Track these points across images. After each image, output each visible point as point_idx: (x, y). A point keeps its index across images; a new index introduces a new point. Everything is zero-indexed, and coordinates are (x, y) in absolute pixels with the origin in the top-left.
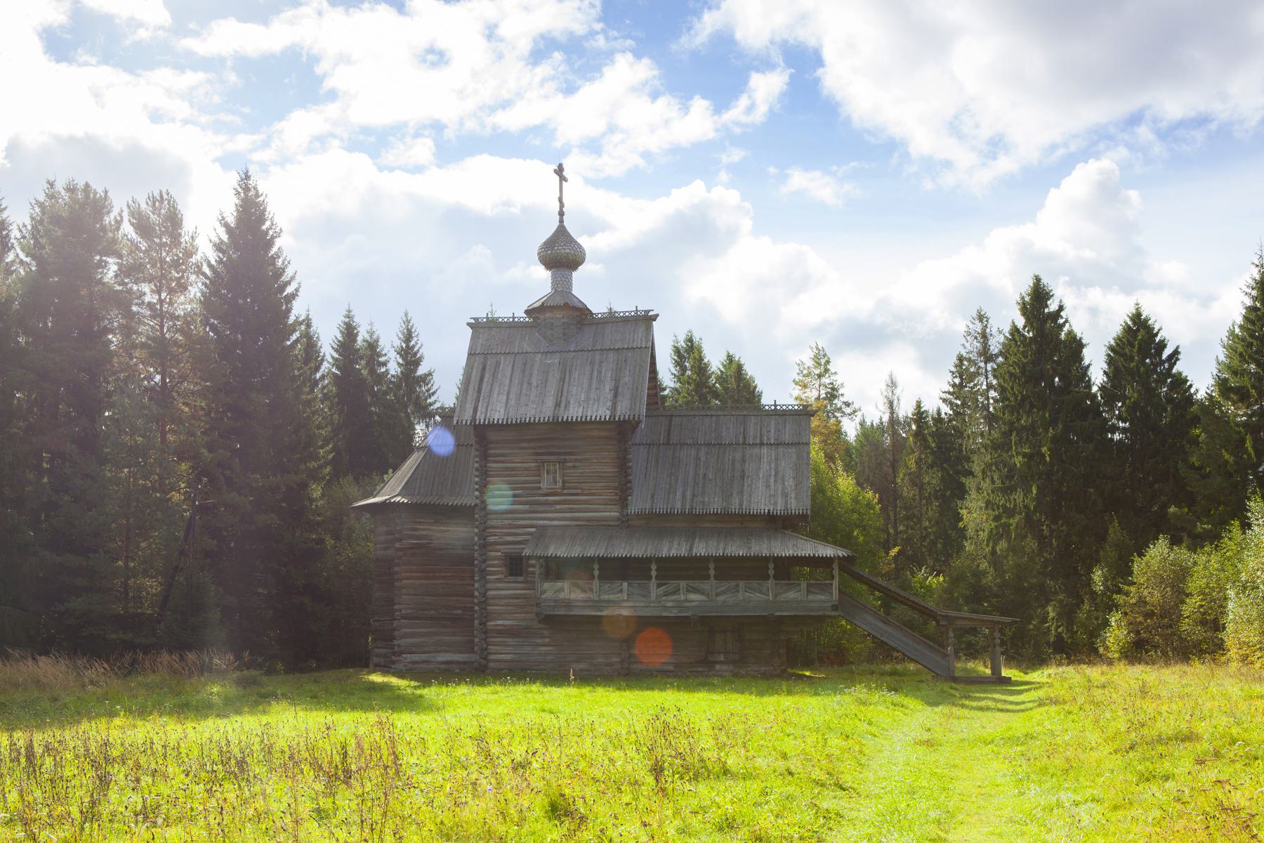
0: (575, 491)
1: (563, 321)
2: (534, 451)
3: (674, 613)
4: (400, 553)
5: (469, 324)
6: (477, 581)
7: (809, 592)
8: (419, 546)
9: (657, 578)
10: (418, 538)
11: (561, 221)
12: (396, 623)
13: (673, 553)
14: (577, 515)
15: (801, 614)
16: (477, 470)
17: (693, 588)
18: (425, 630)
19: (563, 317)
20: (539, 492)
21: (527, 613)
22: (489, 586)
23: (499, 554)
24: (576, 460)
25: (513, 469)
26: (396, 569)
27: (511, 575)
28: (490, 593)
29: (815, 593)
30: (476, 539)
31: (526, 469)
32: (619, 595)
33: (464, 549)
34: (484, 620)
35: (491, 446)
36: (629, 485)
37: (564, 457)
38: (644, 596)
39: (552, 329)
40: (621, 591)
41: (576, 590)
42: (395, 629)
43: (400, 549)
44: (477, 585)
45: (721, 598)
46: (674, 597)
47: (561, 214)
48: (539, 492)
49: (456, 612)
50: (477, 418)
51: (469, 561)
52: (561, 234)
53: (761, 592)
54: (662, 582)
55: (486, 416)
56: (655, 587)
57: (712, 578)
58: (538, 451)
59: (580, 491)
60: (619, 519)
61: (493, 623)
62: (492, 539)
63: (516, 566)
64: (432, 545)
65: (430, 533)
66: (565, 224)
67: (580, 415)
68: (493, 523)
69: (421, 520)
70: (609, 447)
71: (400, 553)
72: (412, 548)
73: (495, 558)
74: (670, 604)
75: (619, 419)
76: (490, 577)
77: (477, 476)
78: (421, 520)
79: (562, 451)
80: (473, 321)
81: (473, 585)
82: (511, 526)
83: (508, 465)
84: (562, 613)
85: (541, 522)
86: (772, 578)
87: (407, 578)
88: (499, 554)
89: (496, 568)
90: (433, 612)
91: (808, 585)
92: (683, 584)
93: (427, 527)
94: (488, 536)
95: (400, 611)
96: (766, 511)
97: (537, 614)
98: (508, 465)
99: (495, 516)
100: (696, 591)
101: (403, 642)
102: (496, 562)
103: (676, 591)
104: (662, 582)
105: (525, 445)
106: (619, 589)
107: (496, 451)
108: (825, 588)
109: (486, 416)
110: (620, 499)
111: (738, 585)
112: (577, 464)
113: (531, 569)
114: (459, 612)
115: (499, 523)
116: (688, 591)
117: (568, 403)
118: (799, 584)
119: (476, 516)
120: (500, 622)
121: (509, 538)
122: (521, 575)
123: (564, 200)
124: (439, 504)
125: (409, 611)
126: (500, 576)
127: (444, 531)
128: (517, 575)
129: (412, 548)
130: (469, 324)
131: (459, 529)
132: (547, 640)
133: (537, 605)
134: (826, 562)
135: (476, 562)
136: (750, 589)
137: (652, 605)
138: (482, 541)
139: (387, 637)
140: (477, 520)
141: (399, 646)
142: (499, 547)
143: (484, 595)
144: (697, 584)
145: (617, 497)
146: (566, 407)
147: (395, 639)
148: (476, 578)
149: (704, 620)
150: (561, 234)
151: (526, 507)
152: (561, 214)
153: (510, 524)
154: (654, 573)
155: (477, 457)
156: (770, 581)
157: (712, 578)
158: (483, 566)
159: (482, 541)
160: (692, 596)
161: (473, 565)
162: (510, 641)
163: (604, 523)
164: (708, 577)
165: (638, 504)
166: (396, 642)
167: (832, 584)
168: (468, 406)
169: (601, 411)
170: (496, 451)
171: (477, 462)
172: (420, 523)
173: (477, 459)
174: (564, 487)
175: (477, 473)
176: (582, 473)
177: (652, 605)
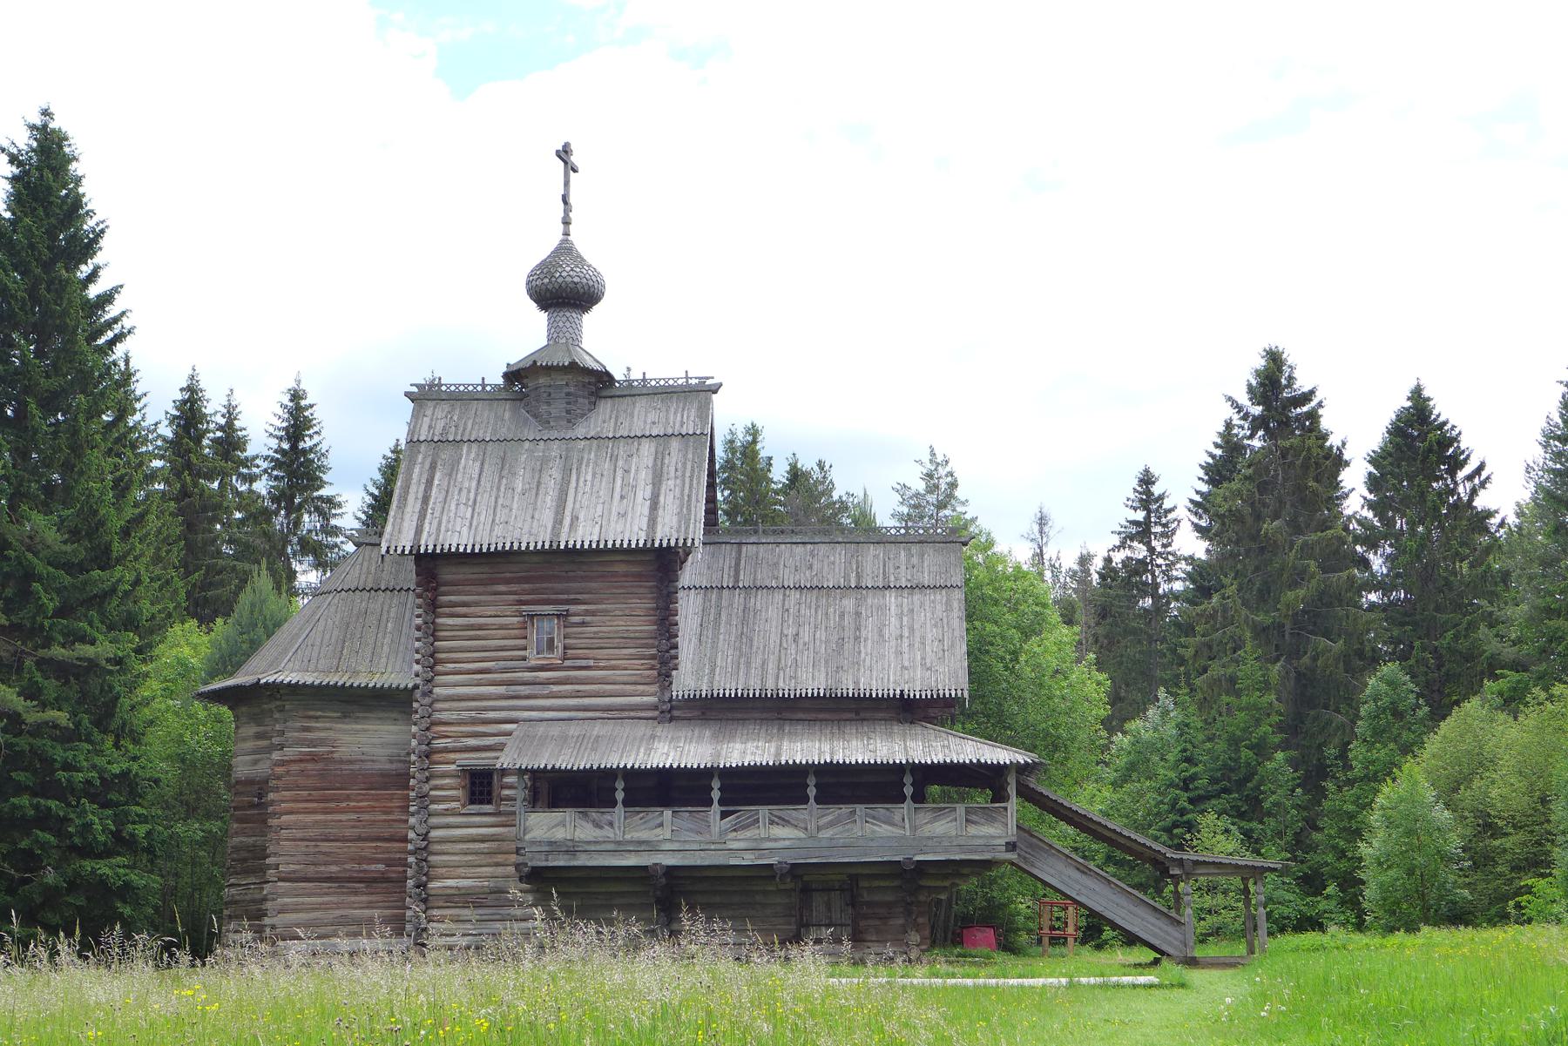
0: (583, 663)
1: (566, 390)
2: (516, 597)
3: (748, 859)
4: (280, 770)
5: (407, 394)
6: (413, 814)
8: (314, 758)
9: (721, 802)
10: (312, 743)
11: (566, 234)
12: (267, 888)
13: (748, 760)
14: (587, 701)
15: (957, 857)
16: (418, 628)
17: (780, 818)
18: (320, 900)
19: (567, 385)
21: (497, 865)
22: (434, 821)
23: (453, 767)
24: (587, 613)
25: (480, 627)
27: (472, 802)
28: (434, 834)
30: (414, 743)
31: (502, 627)
32: (658, 831)
33: (391, 762)
34: (424, 878)
35: (443, 589)
36: (673, 652)
37: (567, 607)
39: (549, 404)
40: (661, 825)
41: (584, 824)
42: (265, 899)
43: (282, 763)
46: (748, 834)
47: (566, 222)
49: (373, 867)
50: (423, 542)
51: (400, 780)
53: (893, 825)
54: (732, 808)
55: (437, 539)
56: (718, 817)
57: (812, 800)
58: (524, 597)
59: (591, 663)
60: (655, 708)
61: (439, 884)
62: (440, 743)
63: (481, 786)
64: (335, 755)
65: (331, 734)
67: (595, 538)
68: (444, 716)
69: (319, 713)
70: (642, 590)
71: (280, 770)
72: (301, 761)
73: (444, 775)
75: (661, 544)
76: (435, 806)
77: (418, 640)
78: (319, 713)
80: (415, 389)
82: (474, 722)
83: (472, 621)
84: (562, 863)
85: (526, 714)
87: (291, 813)
88: (453, 767)
89: (449, 792)
90: (334, 868)
91: (968, 811)
93: (328, 725)
94: (434, 738)
95: (277, 866)
96: (898, 692)
97: (517, 866)
98: (472, 621)
100: (785, 822)
101: (279, 920)
102: (447, 781)
104: (732, 808)
105: (502, 588)
106: (658, 821)
107: (452, 598)
109: (437, 539)
110: (659, 675)
112: (588, 619)
113: (506, 792)
114: (381, 867)
115: (454, 716)
116: (772, 822)
117: (575, 519)
119: (415, 705)
120: (450, 883)
121: (472, 742)
122: (489, 802)
123: (572, 200)
124: (351, 686)
125: (292, 867)
126: (454, 805)
127: (358, 731)
128: (481, 802)
129: (301, 761)
130: (407, 394)
133: (518, 851)
134: (998, 770)
135: (412, 782)
136: (874, 818)
138: (424, 747)
139: (255, 914)
141: (273, 927)
142: (452, 756)
143: (425, 837)
144: (788, 811)
145: (655, 673)
146: (571, 525)
147: (266, 915)
148: (412, 809)
149: (796, 871)
150: (565, 249)
151: (501, 690)
152: (566, 222)
154: (716, 795)
155: (419, 607)
156: (905, 805)
157: (812, 800)
158: (426, 787)
159: (424, 747)
160: (778, 831)
161: (407, 787)
162: (466, 913)
163: (632, 714)
164: (805, 800)
165: (688, 680)
166: (267, 921)
167: (1006, 809)
168: (406, 524)
169: (630, 530)
170: (452, 598)
171: (419, 616)
172: (317, 718)
173: (420, 611)
175: (418, 634)
176: (595, 633)
177: (713, 847)
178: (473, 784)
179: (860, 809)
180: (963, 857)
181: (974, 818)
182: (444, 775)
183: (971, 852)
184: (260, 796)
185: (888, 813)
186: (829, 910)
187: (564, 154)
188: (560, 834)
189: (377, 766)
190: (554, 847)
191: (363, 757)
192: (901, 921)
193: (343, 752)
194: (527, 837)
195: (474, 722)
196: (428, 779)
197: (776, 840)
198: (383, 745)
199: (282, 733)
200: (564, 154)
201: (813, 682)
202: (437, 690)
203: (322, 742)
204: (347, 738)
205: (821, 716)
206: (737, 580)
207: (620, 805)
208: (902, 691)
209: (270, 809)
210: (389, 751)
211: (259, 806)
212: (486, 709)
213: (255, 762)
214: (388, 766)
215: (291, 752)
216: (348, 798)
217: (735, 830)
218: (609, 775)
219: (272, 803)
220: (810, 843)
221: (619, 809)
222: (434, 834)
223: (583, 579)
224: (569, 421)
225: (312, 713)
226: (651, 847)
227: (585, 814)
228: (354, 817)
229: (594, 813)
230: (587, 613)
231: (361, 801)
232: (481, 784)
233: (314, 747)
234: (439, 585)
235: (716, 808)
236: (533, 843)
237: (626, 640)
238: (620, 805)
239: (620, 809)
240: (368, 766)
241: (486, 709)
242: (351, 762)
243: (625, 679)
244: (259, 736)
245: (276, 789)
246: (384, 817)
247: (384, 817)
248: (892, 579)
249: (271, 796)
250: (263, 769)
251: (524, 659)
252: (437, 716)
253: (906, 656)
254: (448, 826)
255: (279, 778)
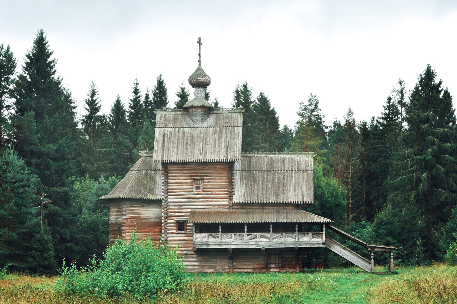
1: (201, 113)
2: (190, 174)
3: (255, 247)
4: (125, 221)
6: (163, 234)
7: (312, 237)
8: (134, 218)
9: (247, 232)
10: (134, 214)
11: (200, 65)
13: (255, 221)
15: (309, 246)
16: (163, 183)
17: (263, 236)
19: (201, 111)
20: (192, 193)
21: (186, 247)
22: (168, 235)
23: (173, 221)
24: (209, 179)
25: (180, 183)
26: (123, 228)
27: (179, 230)
28: (169, 239)
29: (314, 238)
30: (163, 214)
31: (186, 183)
32: (231, 239)
33: (155, 219)
35: (169, 172)
36: (233, 190)
38: (241, 240)
39: (196, 117)
40: (231, 238)
41: (211, 237)
43: (126, 219)
44: (163, 235)
45: (275, 240)
47: (200, 61)
48: (192, 193)
50: (164, 159)
52: (199, 71)
55: (168, 159)
56: (246, 236)
57: (271, 231)
60: (228, 205)
66: (201, 66)
68: (171, 207)
70: (224, 173)
71: (125, 221)
73: (171, 223)
74: (253, 243)
75: (230, 161)
77: (163, 186)
79: (203, 174)
81: (161, 235)
82: (179, 209)
86: (297, 231)
88: (173, 221)
89: (172, 227)
91: (312, 234)
92: (258, 234)
93: (138, 209)
94: (168, 213)
96: (294, 202)
99: (171, 204)
100: (264, 237)
103: (255, 237)
105: (186, 172)
106: (231, 236)
107: (172, 175)
108: (319, 236)
109: (168, 159)
110: (229, 196)
111: (282, 235)
112: (210, 181)
113: (188, 228)
115: (173, 207)
116: (261, 237)
118: (309, 234)
119: (163, 204)
122: (184, 230)
123: (201, 55)
124: (145, 199)
127: (146, 210)
128: (181, 230)
129: (131, 218)
131: (154, 209)
132: (195, 259)
133: (193, 244)
135: (162, 225)
136: (288, 236)
137: (245, 243)
138: (166, 216)
140: (163, 206)
142: (173, 218)
148: (163, 232)
149: (267, 249)
150: (199, 71)
151: (186, 200)
152: (200, 61)
153: (178, 208)
154: (246, 230)
155: (163, 177)
156: (296, 233)
157: (271, 231)
158: (166, 226)
159: (166, 216)
160: (262, 240)
161: (161, 226)
163: (222, 207)
164: (269, 231)
167: (322, 234)
169: (222, 158)
170: (172, 175)
171: (163, 179)
172: (135, 207)
173: (163, 178)
174: (203, 191)
175: (163, 184)
177: (245, 243)
178: (179, 225)
179: (284, 234)
180: (311, 246)
181: (314, 236)
182: (171, 223)
183: (313, 245)
184: (119, 228)
185: (291, 235)
186: (275, 260)
187: (199, 42)
188: (205, 240)
189: (152, 220)
190: (203, 243)
191: (148, 218)
192: (294, 263)
193: (142, 216)
194: (196, 240)
195: (179, 209)
196: (167, 224)
197: (262, 242)
198: (153, 214)
199: (125, 211)
200: (199, 42)
201: (272, 199)
202: (169, 200)
203: (136, 213)
204: (143, 212)
205: (274, 208)
206: (250, 168)
207: (220, 232)
208: (295, 202)
209: (123, 231)
210: (154, 216)
211: (119, 230)
212: (182, 205)
213: (117, 218)
214: (154, 220)
215: (128, 216)
216: (144, 229)
217: (251, 239)
218: (218, 224)
219: (123, 230)
220: (270, 243)
221: (220, 234)
222: (169, 239)
223: (208, 169)
224: (202, 122)
225: (133, 205)
226: (229, 244)
227: (211, 235)
228: (146, 234)
229: (213, 234)
230: (209, 179)
231: (147, 229)
232: (181, 225)
233: (134, 215)
234: (169, 171)
235: (246, 233)
236: (197, 242)
237: (220, 186)
238: (220, 232)
239: (220, 234)
240: (149, 220)
241: (182, 205)
242: (144, 219)
243: (220, 197)
244: (118, 211)
245: (124, 226)
246: (154, 234)
247: (154, 234)
248: (293, 168)
249: (123, 228)
250: (120, 220)
251: (192, 191)
252: (169, 207)
253: (297, 191)
254: (172, 237)
255: (125, 223)
